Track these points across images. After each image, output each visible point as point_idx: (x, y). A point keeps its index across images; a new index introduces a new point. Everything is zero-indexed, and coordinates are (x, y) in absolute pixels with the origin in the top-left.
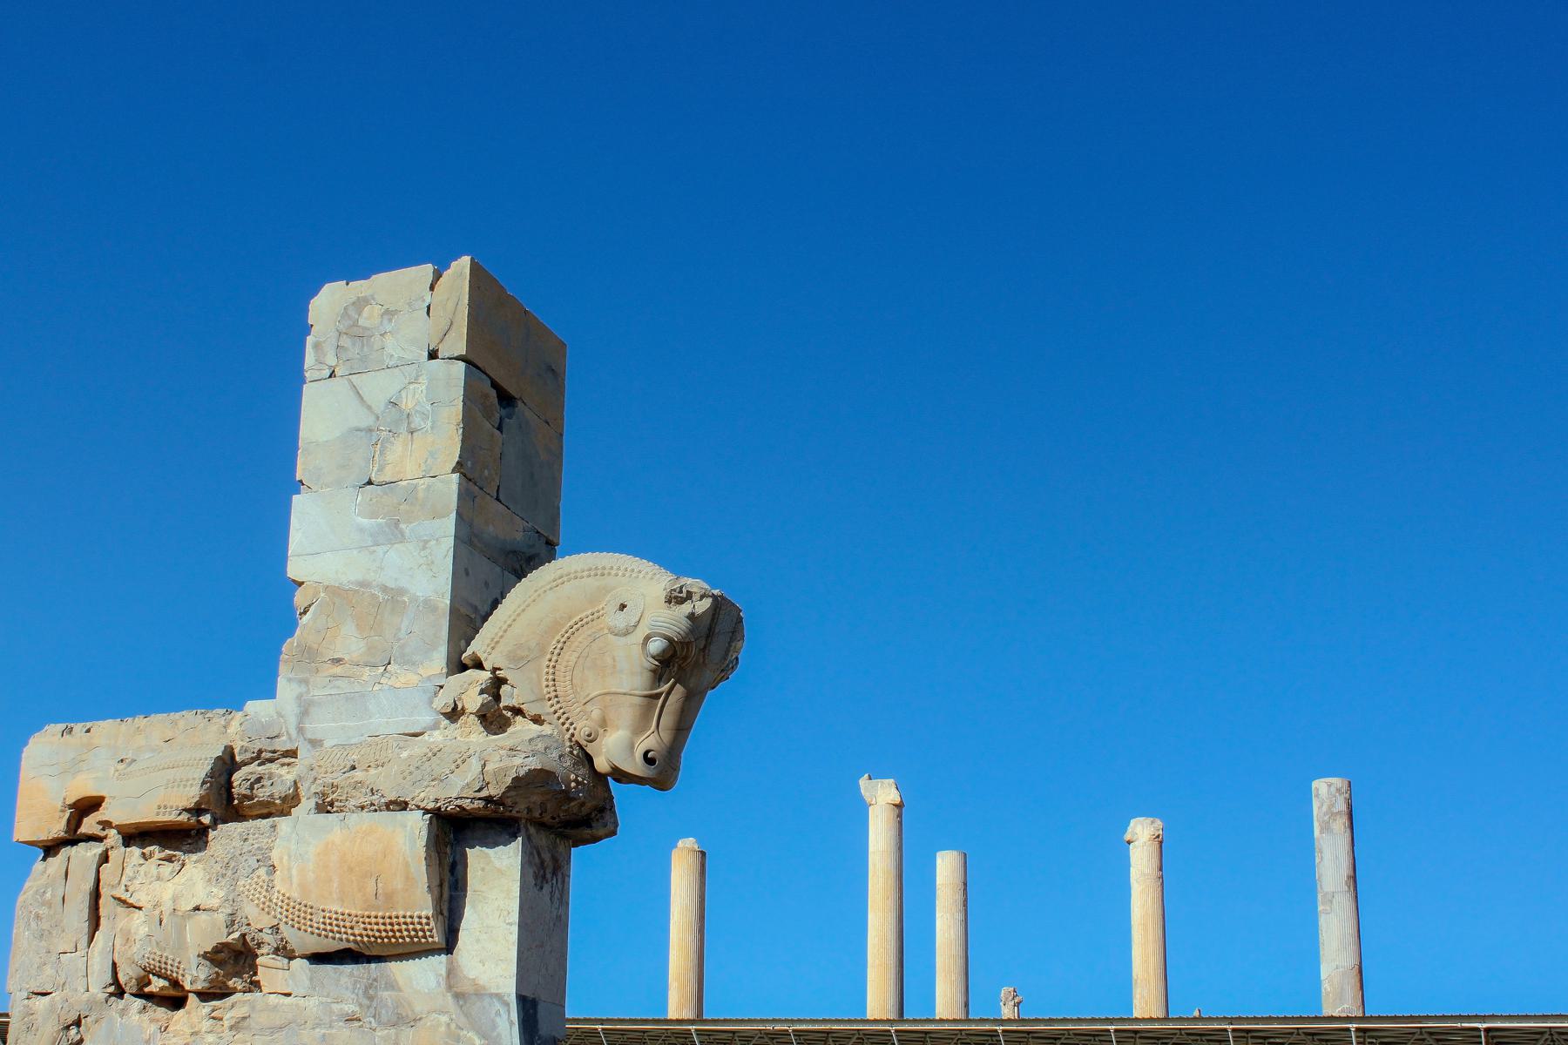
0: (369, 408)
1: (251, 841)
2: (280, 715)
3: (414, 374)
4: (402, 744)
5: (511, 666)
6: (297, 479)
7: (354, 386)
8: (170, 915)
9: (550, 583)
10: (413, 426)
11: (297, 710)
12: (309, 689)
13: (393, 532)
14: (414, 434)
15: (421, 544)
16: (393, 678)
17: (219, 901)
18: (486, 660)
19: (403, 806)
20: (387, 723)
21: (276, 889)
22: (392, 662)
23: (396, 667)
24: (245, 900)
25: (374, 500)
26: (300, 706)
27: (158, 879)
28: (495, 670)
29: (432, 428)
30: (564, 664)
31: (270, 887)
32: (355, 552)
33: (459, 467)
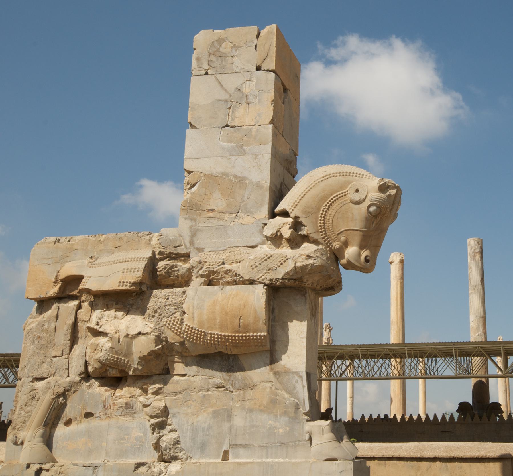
0: (226, 91)
1: (170, 299)
2: (180, 236)
3: (249, 77)
4: (248, 251)
5: (304, 216)
6: (188, 121)
7: (218, 80)
8: (124, 337)
9: (321, 178)
10: (249, 101)
11: (189, 234)
12: (196, 224)
13: (240, 150)
14: (250, 105)
15: (254, 156)
16: (241, 219)
17: (151, 329)
18: (291, 213)
19: (252, 282)
20: (238, 241)
21: (185, 323)
22: (240, 212)
23: (242, 214)
24: (166, 328)
25: (229, 134)
26: (191, 231)
27: (115, 318)
28: (296, 217)
29: (259, 102)
30: (329, 215)
31: (182, 323)
32: (220, 158)
33: (272, 122)
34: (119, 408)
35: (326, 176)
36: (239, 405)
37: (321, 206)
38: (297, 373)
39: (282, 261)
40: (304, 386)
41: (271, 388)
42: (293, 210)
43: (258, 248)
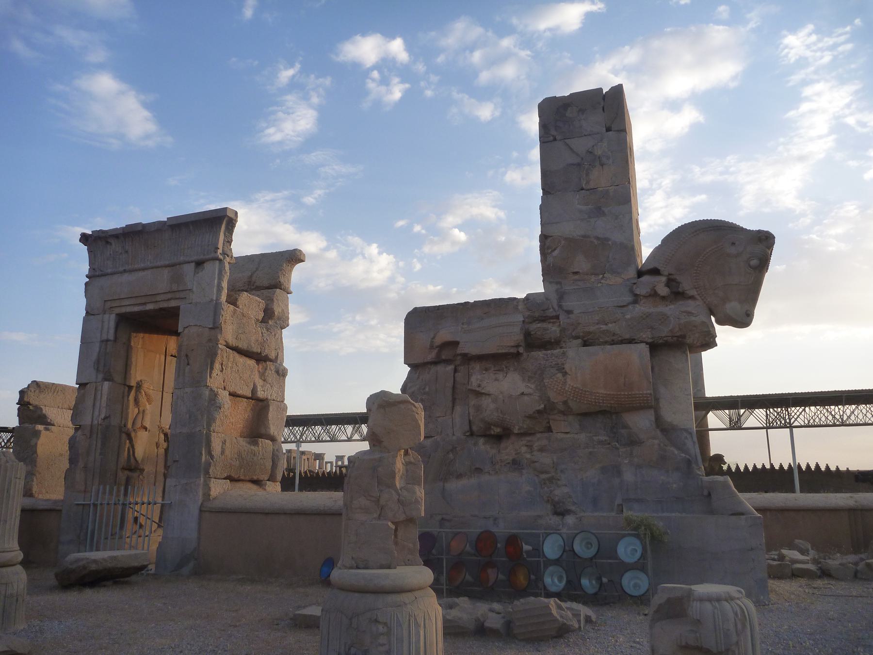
16: (608, 280)
34: (507, 464)
35: (696, 231)
36: (627, 461)
38: (686, 430)
40: (694, 443)
41: (659, 445)
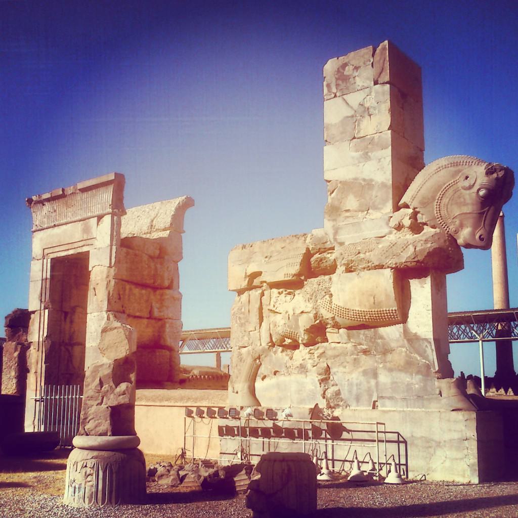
37: (436, 195)
39: (405, 247)
42: (412, 202)
43: (386, 237)
